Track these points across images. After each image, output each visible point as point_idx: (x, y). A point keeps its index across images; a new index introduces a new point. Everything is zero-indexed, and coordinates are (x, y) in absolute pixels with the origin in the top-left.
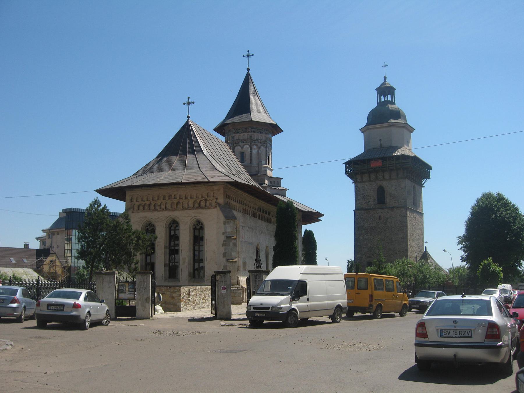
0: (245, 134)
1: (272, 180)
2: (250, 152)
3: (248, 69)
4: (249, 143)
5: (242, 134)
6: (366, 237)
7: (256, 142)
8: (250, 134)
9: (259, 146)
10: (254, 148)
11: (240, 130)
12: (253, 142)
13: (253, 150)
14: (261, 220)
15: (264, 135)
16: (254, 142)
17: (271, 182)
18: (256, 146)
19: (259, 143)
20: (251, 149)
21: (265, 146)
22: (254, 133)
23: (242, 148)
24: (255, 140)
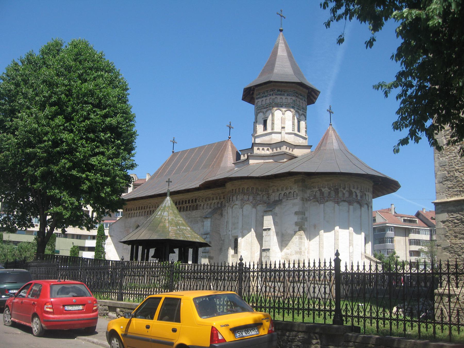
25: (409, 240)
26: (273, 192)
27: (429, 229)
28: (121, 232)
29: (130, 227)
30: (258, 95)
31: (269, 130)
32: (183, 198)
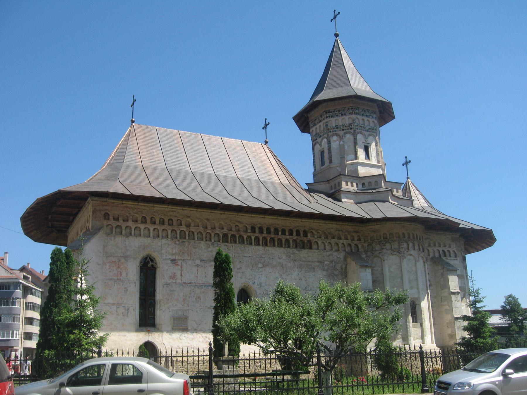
1: (366, 182)
2: (328, 146)
3: (337, 35)
5: (318, 126)
7: (335, 131)
8: (326, 121)
9: (341, 135)
10: (334, 140)
11: (316, 120)
12: (330, 132)
13: (332, 143)
15: (346, 117)
16: (333, 131)
17: (363, 184)
18: (337, 136)
19: (340, 130)
20: (329, 143)
21: (351, 132)
22: (331, 119)
23: (320, 145)
24: (333, 128)
25: (26, 303)
26: (430, 246)
27: (41, 290)
28: (99, 264)
29: (126, 258)
30: (356, 109)
31: (374, 161)
32: (278, 225)
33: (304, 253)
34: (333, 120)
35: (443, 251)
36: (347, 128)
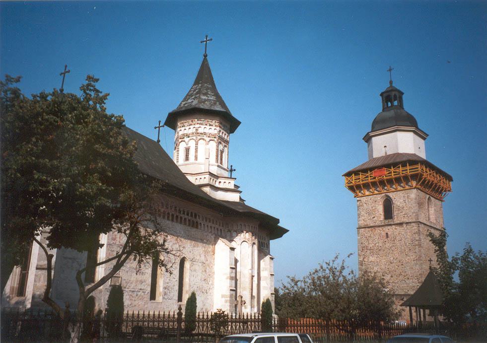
0: (191, 127)
4: (194, 138)
6: (371, 259)
14: (172, 220)
20: (197, 144)
22: (201, 126)
24: (202, 134)
33: (193, 231)
34: (203, 127)
35: (262, 242)
36: (212, 136)
